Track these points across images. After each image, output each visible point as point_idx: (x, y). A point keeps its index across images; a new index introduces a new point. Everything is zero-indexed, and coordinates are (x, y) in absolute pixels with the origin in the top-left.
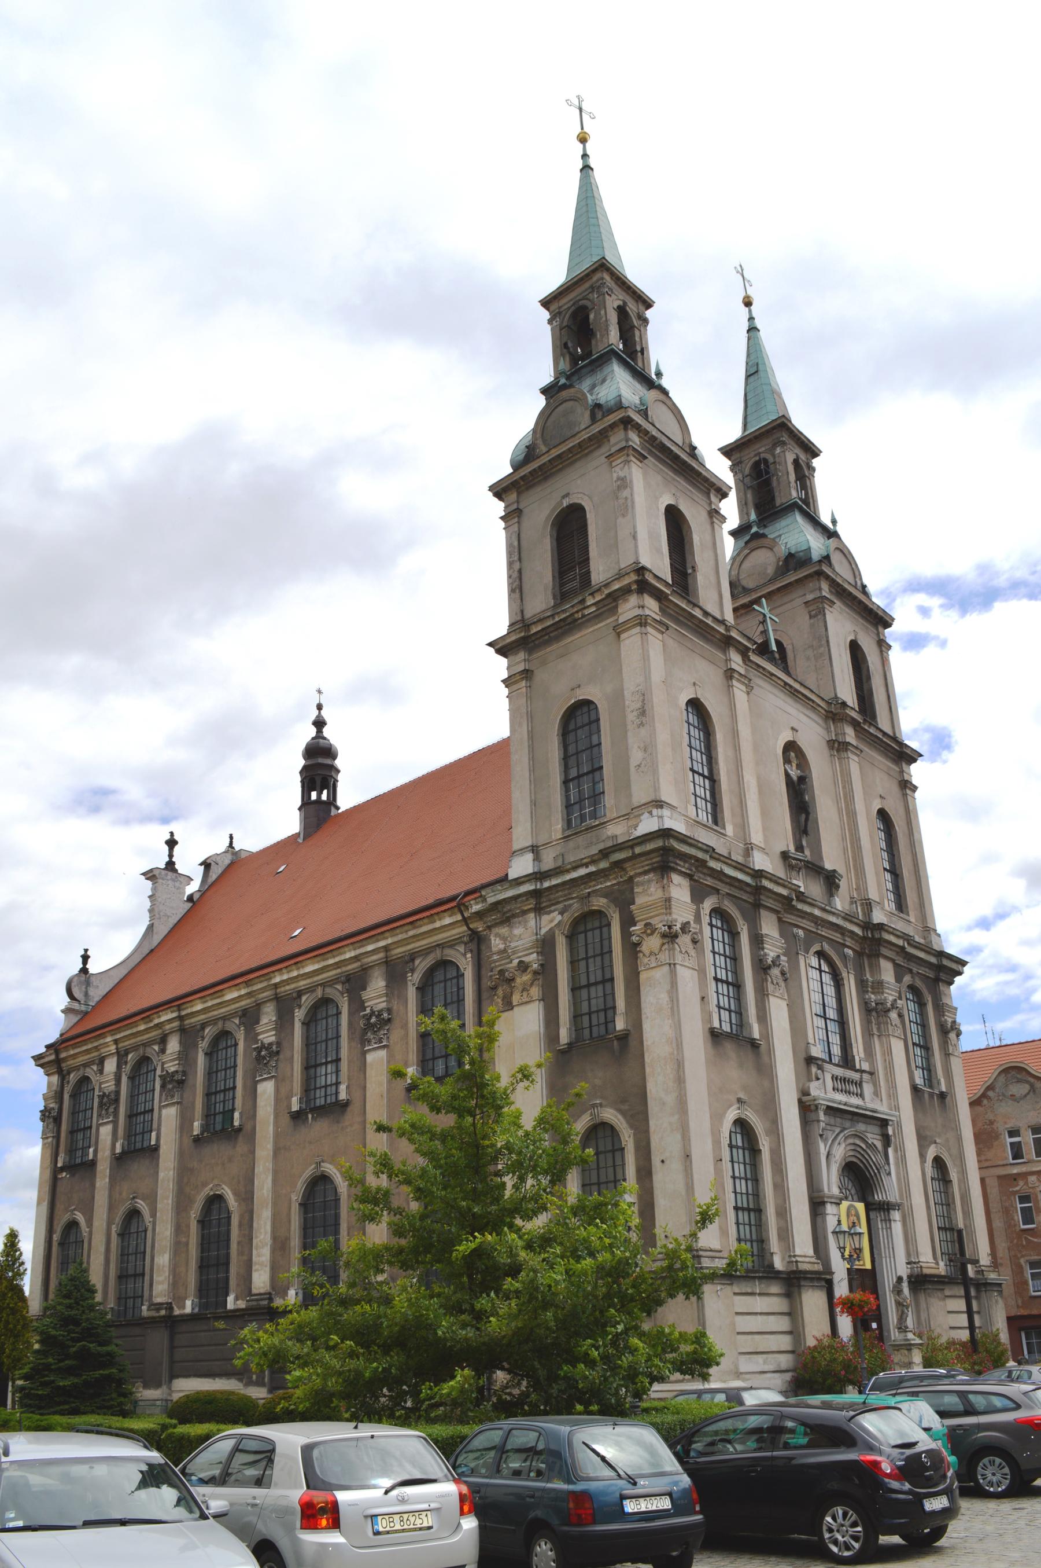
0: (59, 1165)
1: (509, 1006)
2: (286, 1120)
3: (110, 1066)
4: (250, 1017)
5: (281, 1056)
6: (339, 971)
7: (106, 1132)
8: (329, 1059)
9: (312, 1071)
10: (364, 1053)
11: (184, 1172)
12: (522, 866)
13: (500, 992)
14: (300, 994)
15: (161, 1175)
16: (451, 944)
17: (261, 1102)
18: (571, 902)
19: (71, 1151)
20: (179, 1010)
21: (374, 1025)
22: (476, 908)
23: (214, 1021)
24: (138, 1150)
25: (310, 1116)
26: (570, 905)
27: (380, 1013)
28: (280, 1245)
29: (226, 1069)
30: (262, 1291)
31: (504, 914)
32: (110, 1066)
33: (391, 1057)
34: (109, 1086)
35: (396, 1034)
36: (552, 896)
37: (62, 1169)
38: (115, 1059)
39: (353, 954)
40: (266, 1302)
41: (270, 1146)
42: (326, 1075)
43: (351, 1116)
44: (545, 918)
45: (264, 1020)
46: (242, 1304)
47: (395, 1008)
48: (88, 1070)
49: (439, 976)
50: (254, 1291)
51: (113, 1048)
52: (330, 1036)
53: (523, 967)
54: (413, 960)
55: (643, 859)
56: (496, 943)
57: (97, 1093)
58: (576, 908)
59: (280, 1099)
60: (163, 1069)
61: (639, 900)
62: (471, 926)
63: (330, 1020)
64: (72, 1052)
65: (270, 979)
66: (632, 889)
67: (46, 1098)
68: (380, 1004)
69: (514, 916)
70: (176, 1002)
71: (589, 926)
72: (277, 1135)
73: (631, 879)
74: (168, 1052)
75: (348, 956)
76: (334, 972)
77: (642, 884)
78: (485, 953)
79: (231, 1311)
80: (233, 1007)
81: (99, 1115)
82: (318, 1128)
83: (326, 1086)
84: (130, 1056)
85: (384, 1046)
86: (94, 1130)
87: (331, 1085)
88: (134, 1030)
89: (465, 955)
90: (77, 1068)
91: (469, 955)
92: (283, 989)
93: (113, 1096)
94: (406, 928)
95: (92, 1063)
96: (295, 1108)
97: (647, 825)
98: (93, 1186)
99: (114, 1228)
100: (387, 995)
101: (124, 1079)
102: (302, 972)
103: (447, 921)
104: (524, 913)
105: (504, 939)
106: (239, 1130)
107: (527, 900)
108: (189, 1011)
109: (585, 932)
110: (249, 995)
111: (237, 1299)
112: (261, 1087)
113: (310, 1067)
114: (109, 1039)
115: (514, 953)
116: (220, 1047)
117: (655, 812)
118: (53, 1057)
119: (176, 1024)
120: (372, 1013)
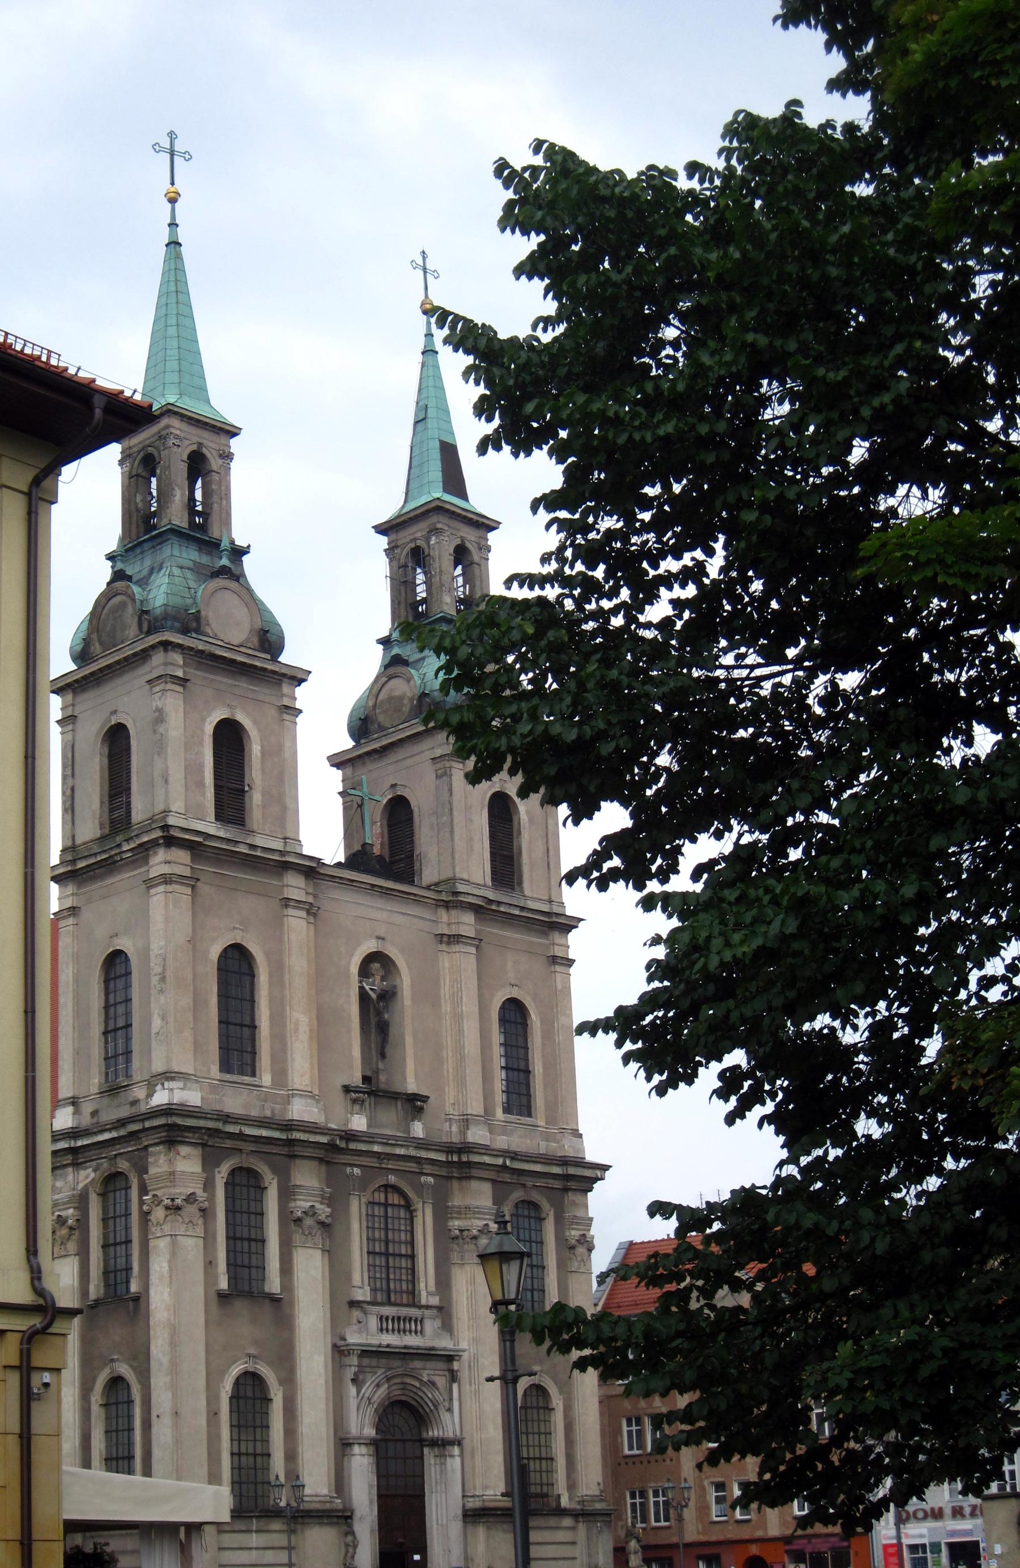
44: (83, 1173)
61: (153, 1171)
73: (146, 1147)
97: (160, 1098)
104: (65, 1166)
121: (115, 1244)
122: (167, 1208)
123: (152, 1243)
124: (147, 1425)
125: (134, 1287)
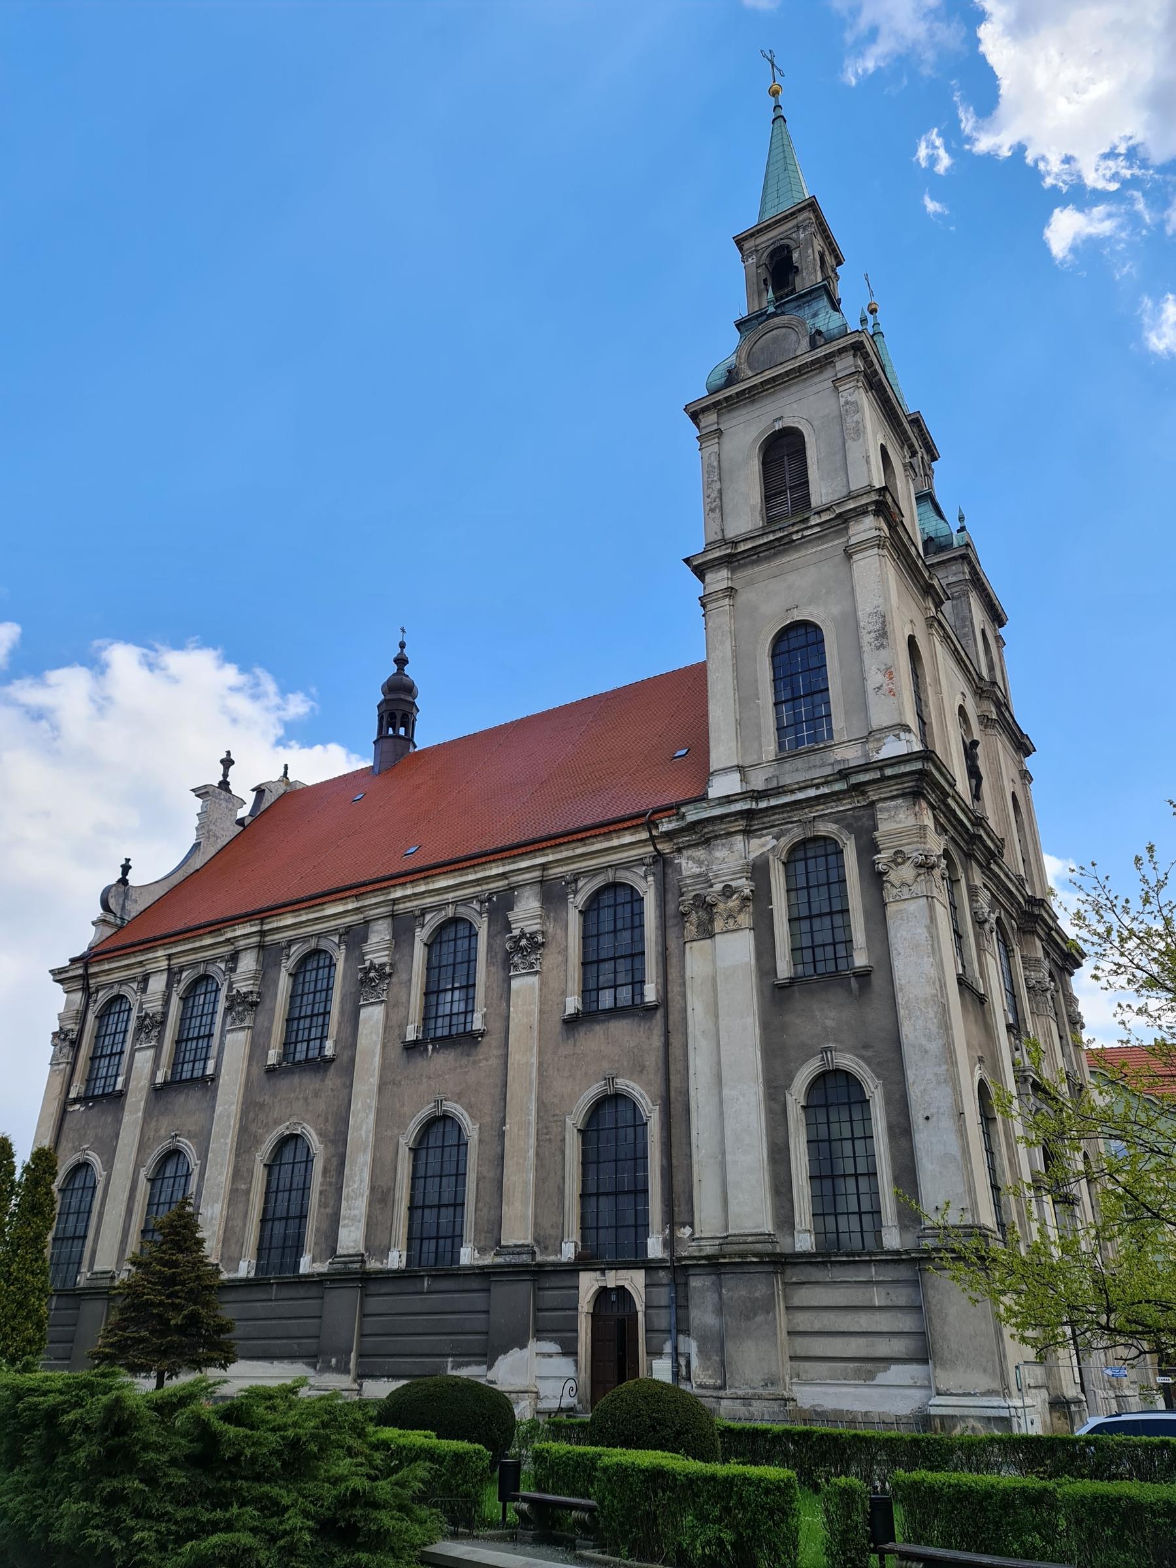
0: (72, 1095)
1: (707, 933)
2: (396, 1050)
3: (157, 984)
4: (355, 937)
5: (394, 979)
6: (478, 889)
7: (144, 1059)
8: (456, 985)
9: (433, 998)
10: (509, 979)
11: (251, 1106)
12: (723, 786)
13: (694, 917)
14: (424, 911)
15: (219, 1109)
16: (627, 865)
17: (363, 1029)
18: (790, 826)
19: (90, 1080)
20: (262, 924)
21: (522, 949)
22: (665, 827)
23: (306, 938)
24: (187, 1081)
25: (430, 1047)
26: (789, 830)
27: (533, 935)
28: (380, 1197)
29: (315, 993)
30: (352, 1252)
31: (703, 834)
32: (157, 984)
33: (543, 984)
34: (154, 1006)
35: (549, 959)
36: (765, 820)
37: (76, 1101)
38: (165, 976)
39: (501, 870)
40: (357, 1265)
41: (374, 1081)
42: (452, 1002)
43: (488, 1050)
44: (755, 842)
45: (374, 939)
46: (322, 1267)
47: (550, 930)
48: (124, 988)
49: (607, 899)
50: (340, 1251)
51: (164, 964)
52: (459, 960)
53: (728, 892)
54: (576, 881)
55: (892, 782)
56: (688, 865)
57: (134, 1014)
58: (796, 834)
59: (390, 1027)
60: (230, 988)
61: (884, 827)
62: (659, 847)
63: (459, 942)
64: (107, 967)
65: (389, 893)
66: (873, 817)
67: (61, 1018)
68: (532, 926)
69: (716, 837)
70: (261, 914)
71: (810, 853)
72: (383, 1068)
74: (238, 970)
75: (494, 872)
76: (472, 890)
77: (888, 810)
78: (672, 877)
79: (305, 1276)
80: (333, 923)
81: (136, 1039)
82: (441, 1061)
83: (451, 1015)
84: (184, 974)
85: (536, 973)
86: (126, 1057)
87: (458, 1014)
88: (197, 944)
89: (646, 877)
90: (110, 985)
91: (651, 878)
92: (402, 906)
93: (158, 1018)
94: (574, 845)
95: (133, 979)
96: (411, 1036)
98: (119, 1121)
99: (143, 1172)
100: (541, 917)
101: (175, 1002)
102: (431, 887)
103: (628, 839)
104: (730, 834)
105: (700, 863)
106: (332, 1060)
107: (736, 820)
108: (275, 925)
109: (806, 859)
110: (357, 910)
111: (314, 1261)
112: (364, 1013)
113: (431, 992)
114: (160, 953)
115: (716, 876)
116: (309, 968)
117: (902, 735)
118: (81, 971)
119: (255, 940)
120: (523, 935)
121: (819, 914)
122: (920, 866)
123: (891, 909)
124: (902, 1130)
125: (860, 960)
